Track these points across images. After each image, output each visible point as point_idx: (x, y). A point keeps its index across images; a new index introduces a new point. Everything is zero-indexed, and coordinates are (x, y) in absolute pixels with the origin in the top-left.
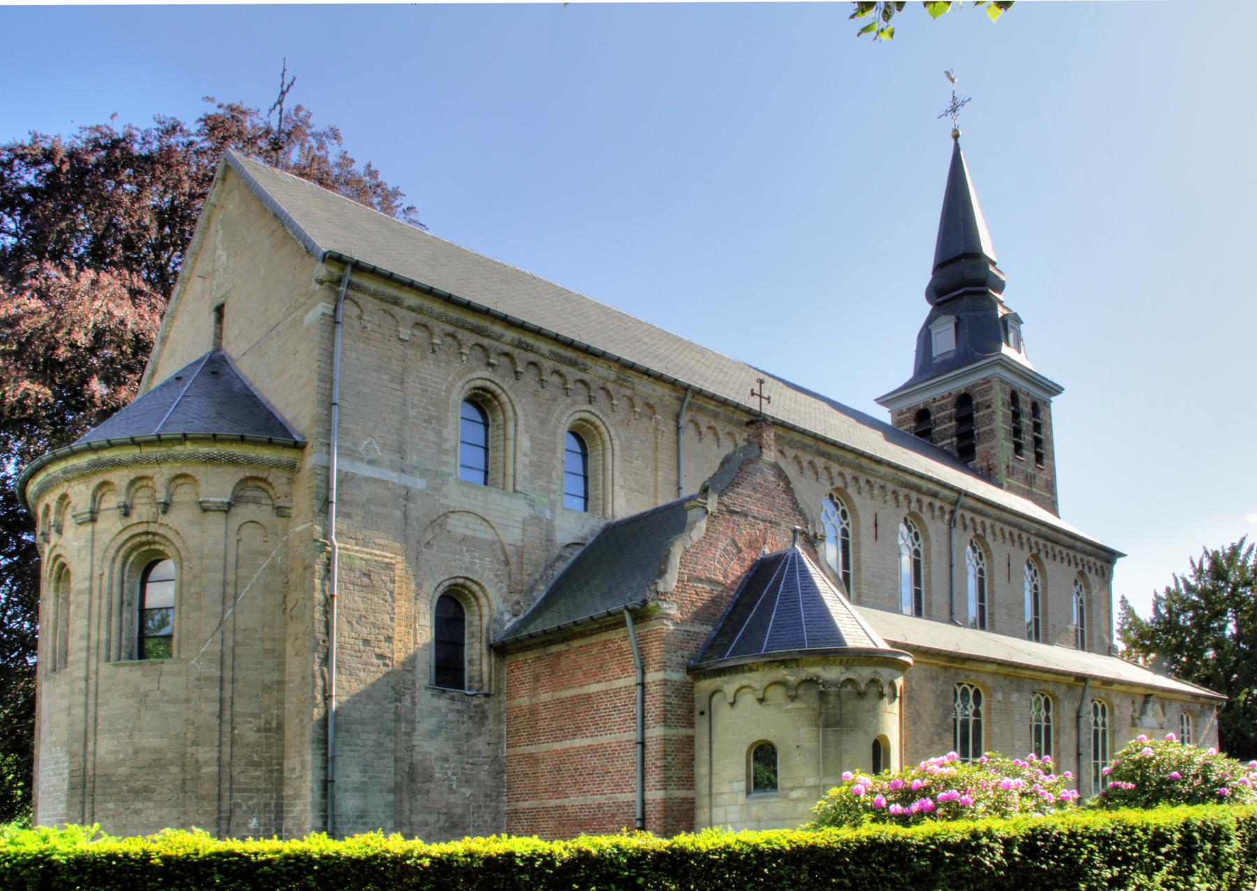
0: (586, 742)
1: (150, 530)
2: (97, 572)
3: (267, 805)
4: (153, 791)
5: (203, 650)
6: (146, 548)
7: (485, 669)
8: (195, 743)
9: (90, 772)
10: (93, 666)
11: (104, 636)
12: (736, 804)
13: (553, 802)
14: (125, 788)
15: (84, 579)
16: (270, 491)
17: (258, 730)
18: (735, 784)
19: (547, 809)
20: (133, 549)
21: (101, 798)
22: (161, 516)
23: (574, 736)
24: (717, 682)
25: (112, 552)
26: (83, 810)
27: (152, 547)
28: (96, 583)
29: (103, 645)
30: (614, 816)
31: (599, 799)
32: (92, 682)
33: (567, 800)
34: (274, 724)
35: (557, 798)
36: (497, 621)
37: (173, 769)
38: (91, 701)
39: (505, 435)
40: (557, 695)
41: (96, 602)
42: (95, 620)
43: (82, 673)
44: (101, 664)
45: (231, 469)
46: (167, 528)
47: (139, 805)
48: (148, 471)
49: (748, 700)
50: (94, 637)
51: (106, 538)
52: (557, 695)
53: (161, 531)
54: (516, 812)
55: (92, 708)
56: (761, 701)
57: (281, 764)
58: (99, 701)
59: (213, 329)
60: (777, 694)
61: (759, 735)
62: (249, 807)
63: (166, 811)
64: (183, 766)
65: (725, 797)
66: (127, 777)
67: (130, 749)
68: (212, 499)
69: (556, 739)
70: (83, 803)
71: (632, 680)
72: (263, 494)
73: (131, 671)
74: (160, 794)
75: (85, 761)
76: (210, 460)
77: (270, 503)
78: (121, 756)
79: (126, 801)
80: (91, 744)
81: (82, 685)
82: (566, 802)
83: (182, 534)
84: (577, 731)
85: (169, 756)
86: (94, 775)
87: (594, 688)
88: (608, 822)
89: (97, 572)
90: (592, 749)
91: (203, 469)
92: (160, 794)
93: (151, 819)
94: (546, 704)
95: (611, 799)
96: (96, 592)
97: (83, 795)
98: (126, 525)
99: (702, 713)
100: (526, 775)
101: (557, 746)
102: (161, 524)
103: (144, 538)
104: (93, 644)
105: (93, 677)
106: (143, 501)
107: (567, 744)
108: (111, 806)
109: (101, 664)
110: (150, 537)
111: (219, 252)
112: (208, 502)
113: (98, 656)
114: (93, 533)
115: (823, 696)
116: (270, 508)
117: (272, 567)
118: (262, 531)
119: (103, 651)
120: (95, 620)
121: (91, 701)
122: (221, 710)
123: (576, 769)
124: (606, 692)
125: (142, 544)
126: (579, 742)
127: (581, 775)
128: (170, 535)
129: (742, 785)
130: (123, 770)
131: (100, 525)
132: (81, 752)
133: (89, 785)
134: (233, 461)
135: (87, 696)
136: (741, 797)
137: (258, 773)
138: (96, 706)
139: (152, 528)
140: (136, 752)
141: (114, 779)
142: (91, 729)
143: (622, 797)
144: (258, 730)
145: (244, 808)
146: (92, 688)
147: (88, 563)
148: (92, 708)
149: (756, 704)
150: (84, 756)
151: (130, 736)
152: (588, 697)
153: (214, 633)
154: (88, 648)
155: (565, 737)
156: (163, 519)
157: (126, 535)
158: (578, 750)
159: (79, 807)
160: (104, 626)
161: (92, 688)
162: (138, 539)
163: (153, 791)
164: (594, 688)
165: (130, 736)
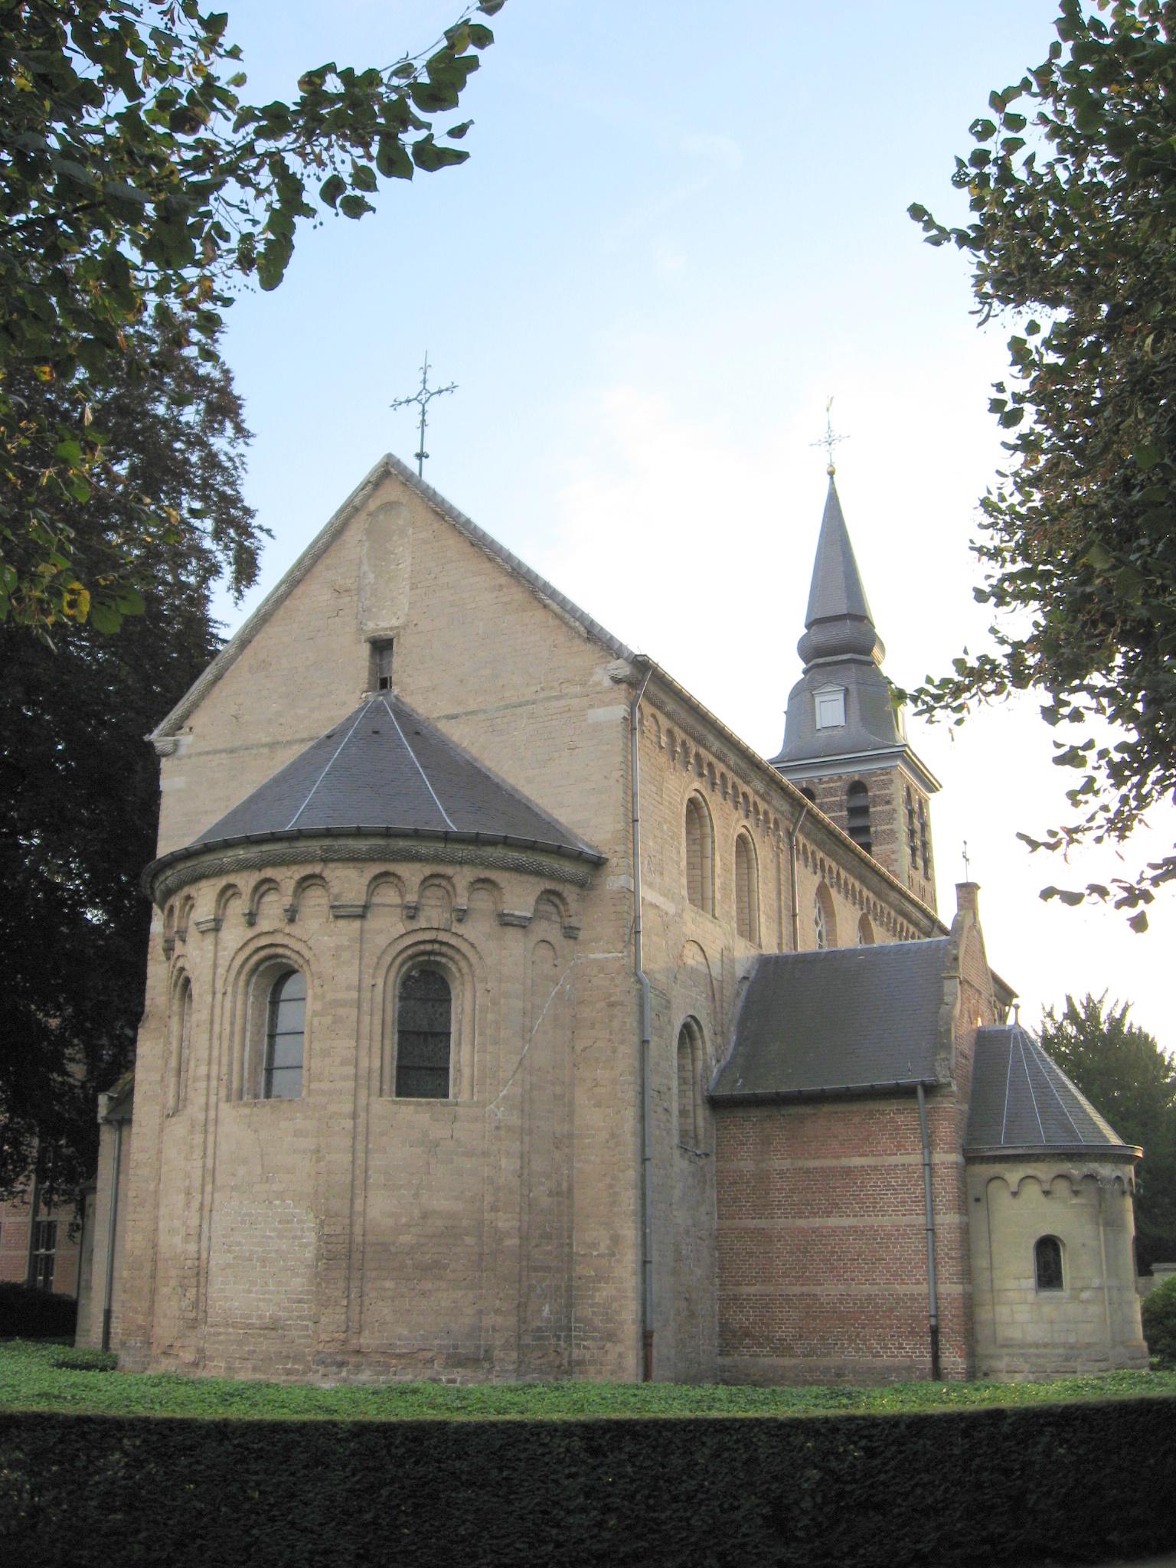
0: (846, 1222)
1: (439, 939)
2: (368, 981)
3: (558, 1288)
4: (445, 1267)
5: (505, 1092)
6: (426, 958)
7: (701, 1123)
8: (494, 1209)
9: (359, 1239)
10: (363, 1100)
11: (377, 1063)
12: (1025, 1302)
13: (797, 1290)
14: (409, 1262)
15: (349, 988)
16: (561, 907)
17: (550, 1194)
18: (1022, 1281)
19: (787, 1299)
20: (411, 957)
21: (374, 1274)
22: (455, 924)
23: (829, 1214)
24: (997, 1169)
25: (388, 959)
26: (348, 1288)
27: (432, 958)
28: (366, 995)
29: (376, 1075)
30: (891, 1310)
31: (874, 1290)
32: (361, 1120)
33: (819, 1288)
34: (565, 1186)
35: (802, 1285)
36: (962, 1112)
37: (469, 1240)
38: (360, 1147)
39: (702, 852)
40: (800, 1163)
41: (366, 1019)
42: (365, 1042)
43: (348, 1108)
44: (373, 1099)
45: (532, 879)
46: (460, 939)
47: (428, 1285)
48: (449, 870)
49: (1032, 1191)
50: (364, 1063)
51: (382, 941)
52: (800, 1163)
53: (453, 941)
54: (735, 1298)
55: (361, 1155)
56: (1046, 1193)
57: (570, 1237)
58: (370, 1146)
59: (368, 664)
60: (1062, 1187)
61: (1045, 1230)
62: (543, 1290)
63: (461, 1293)
64: (480, 1237)
65: (1011, 1294)
66: (412, 1248)
67: (416, 1212)
68: (517, 913)
69: (800, 1215)
70: (348, 1279)
71: (915, 1159)
72: (552, 909)
73: (416, 1112)
74: (453, 1271)
75: (351, 1225)
76: (518, 869)
77: (558, 919)
78: (404, 1220)
79: (409, 1280)
80: (359, 1202)
81: (348, 1124)
82: (818, 1290)
83: (479, 949)
84: (833, 1208)
85: (465, 1223)
86: (364, 1243)
87: (857, 1161)
88: (883, 1317)
89: (368, 981)
90: (854, 1229)
91: (507, 875)
92: (453, 1271)
93: (443, 1304)
94: (781, 1173)
95: (886, 1290)
96: (366, 1007)
97: (349, 1268)
98: (410, 928)
99: (977, 1200)
100: (751, 1254)
101: (801, 1223)
102: (455, 934)
103: (428, 947)
104: (363, 1072)
105: (363, 1115)
106: (433, 902)
107: (817, 1222)
108: (389, 1284)
109: (373, 1099)
110: (436, 946)
111: (365, 568)
112: (512, 915)
113: (369, 1088)
114: (362, 931)
115: (1101, 1192)
116: (557, 926)
117: (560, 995)
118: (551, 954)
119: (376, 1084)
120: (365, 1042)
121: (360, 1147)
122: (353, 1146)
123: (832, 1253)
124: (875, 1168)
125: (423, 953)
126: (833, 1222)
127: (840, 1259)
128: (464, 947)
129: (1032, 1282)
130: (406, 1239)
131: (373, 923)
132: (346, 1212)
133: (357, 1256)
134: (538, 873)
135: (354, 1138)
136: (1031, 1296)
137: (549, 1248)
138: (367, 1151)
139: (443, 937)
140: (425, 1216)
141: (393, 1249)
142: (359, 1182)
143: (916, 1289)
144: (550, 1194)
145: (539, 1291)
146: (361, 1128)
147: (356, 967)
148: (361, 1155)
149: (1042, 1197)
150: (350, 1217)
151: (416, 1195)
152: (848, 1171)
153: (515, 1073)
154: (356, 1077)
155: (815, 1214)
156: (457, 928)
157: (408, 941)
158: (834, 1231)
159: (342, 1284)
160: (377, 1051)
161: (361, 1128)
162: (422, 947)
163: (445, 1267)
164: (857, 1161)
165: (416, 1195)
